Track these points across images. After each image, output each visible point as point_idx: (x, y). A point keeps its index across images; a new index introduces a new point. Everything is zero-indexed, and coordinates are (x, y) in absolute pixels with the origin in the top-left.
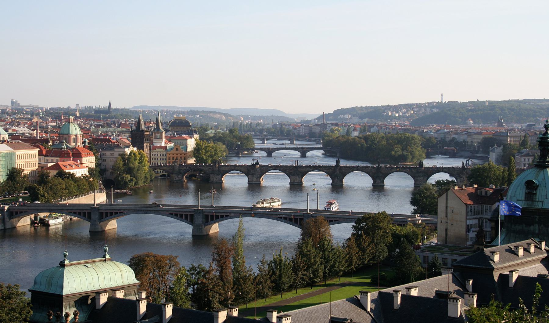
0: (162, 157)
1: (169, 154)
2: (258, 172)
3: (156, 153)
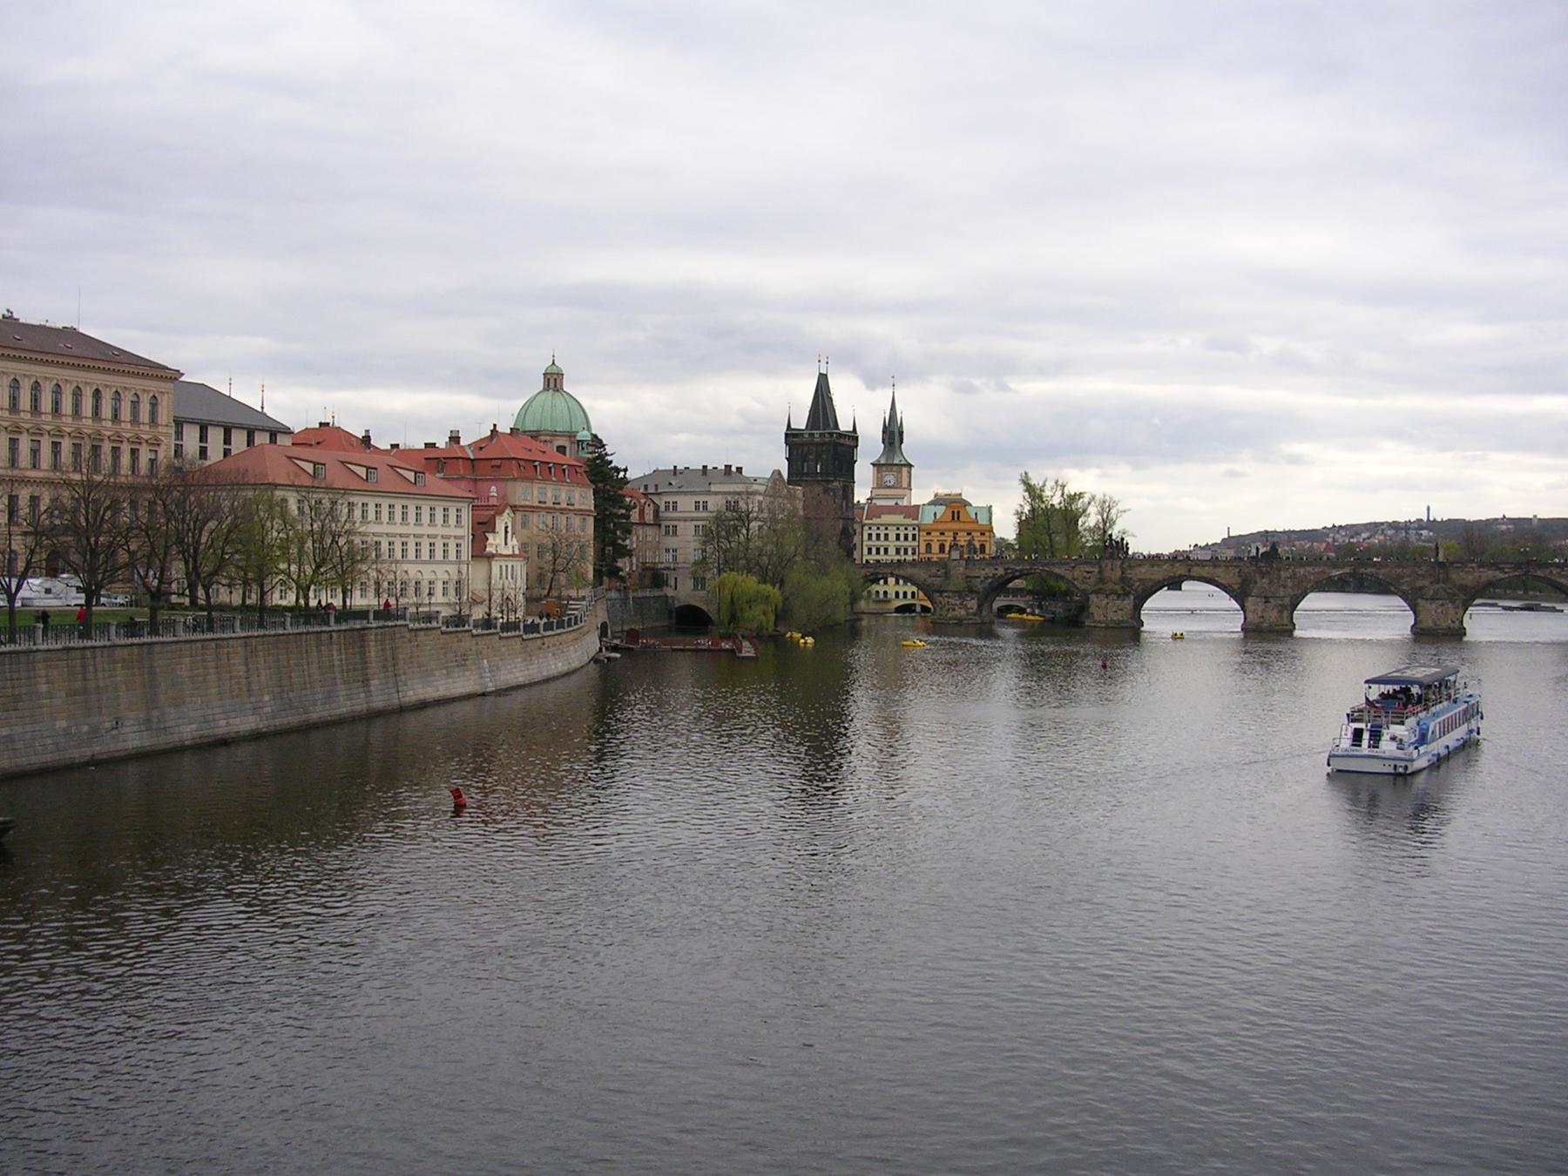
0: (902, 543)
1: (929, 534)
2: (1284, 587)
3: (882, 528)
